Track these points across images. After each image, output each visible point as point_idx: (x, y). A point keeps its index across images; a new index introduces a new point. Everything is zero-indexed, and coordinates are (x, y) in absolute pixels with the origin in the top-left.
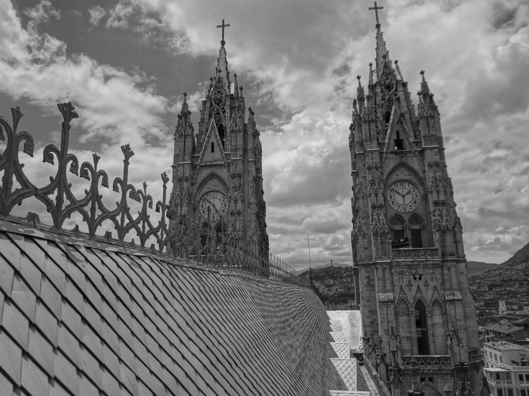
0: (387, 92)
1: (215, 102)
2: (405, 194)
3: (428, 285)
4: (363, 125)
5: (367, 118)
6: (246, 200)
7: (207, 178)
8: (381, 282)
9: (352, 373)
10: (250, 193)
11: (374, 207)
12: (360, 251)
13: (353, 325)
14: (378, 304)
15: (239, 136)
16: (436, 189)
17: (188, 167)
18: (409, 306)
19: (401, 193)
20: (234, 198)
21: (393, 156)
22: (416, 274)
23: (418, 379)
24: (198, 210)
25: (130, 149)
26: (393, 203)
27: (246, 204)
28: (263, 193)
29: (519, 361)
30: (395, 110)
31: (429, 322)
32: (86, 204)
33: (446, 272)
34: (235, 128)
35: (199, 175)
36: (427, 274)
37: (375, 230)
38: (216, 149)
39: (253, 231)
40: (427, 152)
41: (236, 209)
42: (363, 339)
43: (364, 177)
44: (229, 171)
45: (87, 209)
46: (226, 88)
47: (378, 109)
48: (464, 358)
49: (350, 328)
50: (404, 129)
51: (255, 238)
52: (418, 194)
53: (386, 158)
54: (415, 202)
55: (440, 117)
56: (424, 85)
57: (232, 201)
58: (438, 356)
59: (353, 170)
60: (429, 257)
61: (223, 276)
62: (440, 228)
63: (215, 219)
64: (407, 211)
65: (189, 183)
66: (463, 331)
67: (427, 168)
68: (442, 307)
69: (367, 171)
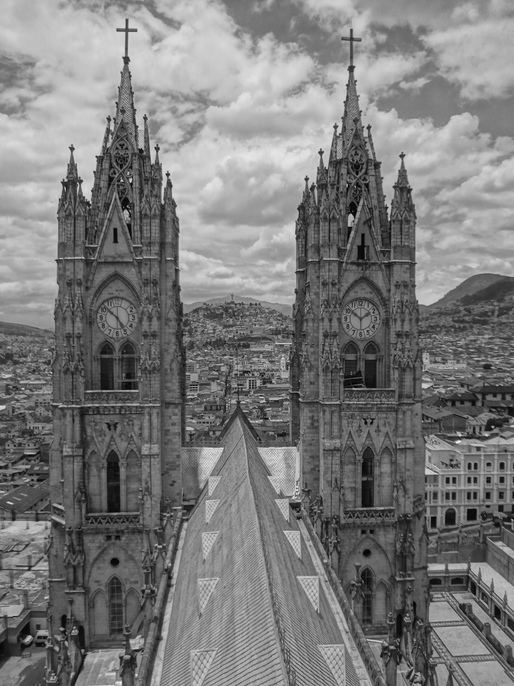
0: (354, 174)
1: (116, 161)
2: (362, 316)
3: (379, 431)
4: (321, 224)
5: (327, 214)
6: (163, 315)
8: (327, 427)
9: (340, 663)
10: (168, 305)
11: (326, 336)
13: (289, 466)
15: (154, 224)
16: (400, 317)
17: (81, 265)
18: (357, 454)
19: (359, 314)
20: (147, 314)
21: (354, 267)
22: (368, 418)
23: (359, 531)
24: (95, 324)
26: (348, 326)
27: (163, 321)
29: (448, 462)
30: (364, 205)
31: (376, 471)
33: (400, 416)
34: (148, 212)
35: (96, 276)
37: (325, 365)
38: (121, 239)
39: (173, 357)
40: (396, 268)
41: (150, 328)
43: (317, 294)
44: (140, 272)
46: (133, 140)
47: (340, 197)
49: (285, 470)
50: (371, 233)
51: (175, 366)
52: (378, 316)
53: (346, 270)
54: (374, 327)
55: (416, 221)
56: (403, 174)
57: (145, 318)
58: (382, 508)
59: (300, 267)
60: (384, 399)
62: (400, 365)
63: (120, 336)
64: (363, 336)
65: (83, 288)
66: (411, 481)
67: (393, 288)
68: (392, 455)
69: (321, 287)
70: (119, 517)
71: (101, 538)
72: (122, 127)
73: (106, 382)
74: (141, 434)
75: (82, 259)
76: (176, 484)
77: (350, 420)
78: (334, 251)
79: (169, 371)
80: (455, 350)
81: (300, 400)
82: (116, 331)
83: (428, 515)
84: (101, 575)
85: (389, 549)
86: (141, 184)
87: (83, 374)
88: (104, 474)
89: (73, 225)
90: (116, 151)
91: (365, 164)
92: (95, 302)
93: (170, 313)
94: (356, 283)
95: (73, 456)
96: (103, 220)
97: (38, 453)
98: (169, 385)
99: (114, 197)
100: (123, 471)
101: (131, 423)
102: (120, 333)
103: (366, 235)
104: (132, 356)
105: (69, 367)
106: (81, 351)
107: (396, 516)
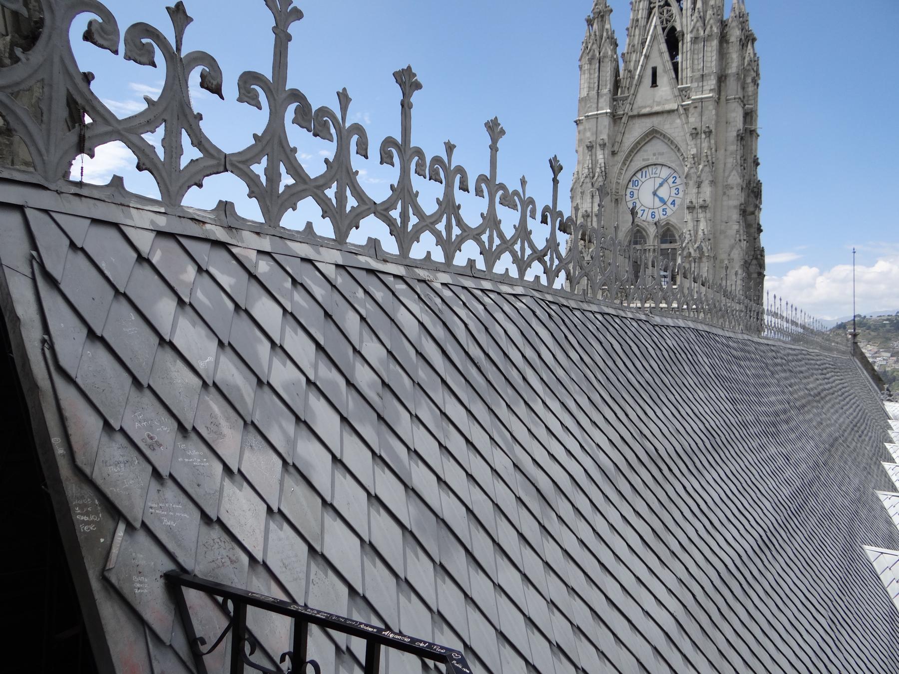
7: (643, 139)
10: (729, 165)
17: (606, 122)
20: (694, 178)
25: (499, 124)
28: (758, 164)
32: (438, 220)
35: (626, 135)
38: (664, 80)
44: (687, 123)
45: (441, 227)
57: (691, 183)
61: (657, 328)
65: (606, 152)
75: (606, 113)
82: (651, 211)
99: (653, 24)
104: (672, 246)
105: (585, 255)
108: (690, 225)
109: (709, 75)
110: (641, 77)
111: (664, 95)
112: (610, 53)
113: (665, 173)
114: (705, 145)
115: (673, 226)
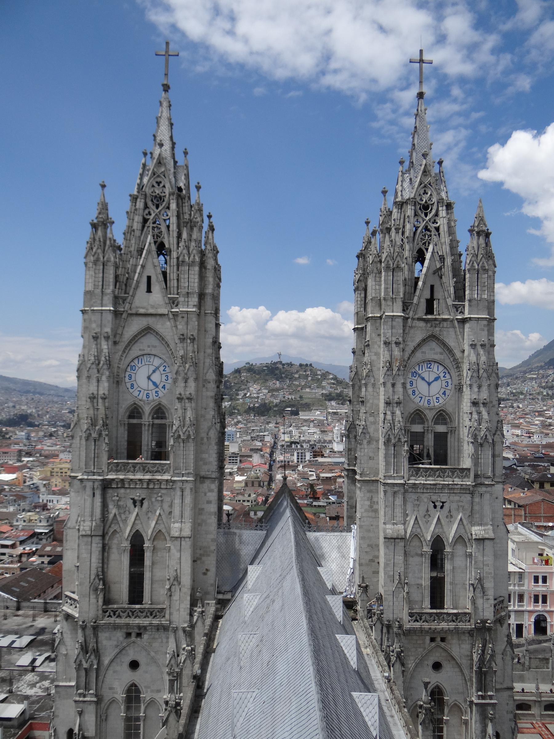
0: (423, 215)
2: (432, 379)
4: (383, 274)
5: (391, 263)
7: (139, 333)
11: (388, 403)
12: (362, 462)
14: (382, 540)
16: (476, 382)
18: (424, 543)
20: (182, 374)
21: (422, 324)
23: (428, 639)
24: (123, 384)
26: (414, 392)
30: (433, 253)
31: (448, 566)
33: (477, 500)
34: (187, 258)
35: (126, 329)
36: (452, 501)
37: (387, 437)
38: (156, 287)
39: (210, 424)
42: (359, 586)
44: (176, 326)
47: (406, 243)
48: (488, 613)
51: (213, 434)
52: (449, 381)
53: (411, 327)
54: (444, 393)
57: (180, 378)
58: (455, 611)
59: (358, 323)
63: (151, 398)
64: (432, 405)
65: (110, 343)
67: (466, 347)
70: (142, 611)
71: (119, 635)
72: (160, 163)
73: (133, 451)
74: (170, 513)
75: (110, 310)
76: (209, 573)
77: (416, 502)
78: (399, 305)
79: (205, 440)
80: (542, 421)
81: (357, 477)
82: (146, 392)
83: (513, 621)
84: (117, 682)
85: (464, 662)
86: (179, 226)
87: (107, 441)
88: (126, 560)
89: (101, 271)
90: (152, 190)
91: (436, 204)
92: (123, 358)
93: (208, 374)
94: (424, 341)
95: (91, 536)
96: (136, 266)
97: (51, 531)
98: (205, 456)
100: (148, 556)
101: (159, 498)
102: (151, 395)
103: (435, 287)
105: (92, 432)
106: (106, 415)
107: (472, 621)
108: (180, 412)
109: (193, 293)
110: (138, 282)
111: (156, 300)
112: (112, 259)
113: (157, 362)
114: (190, 348)
115: (163, 406)
